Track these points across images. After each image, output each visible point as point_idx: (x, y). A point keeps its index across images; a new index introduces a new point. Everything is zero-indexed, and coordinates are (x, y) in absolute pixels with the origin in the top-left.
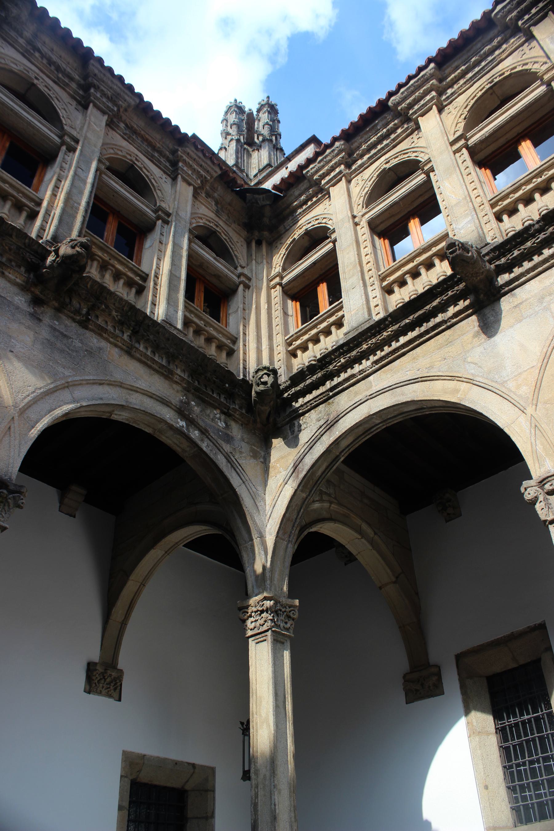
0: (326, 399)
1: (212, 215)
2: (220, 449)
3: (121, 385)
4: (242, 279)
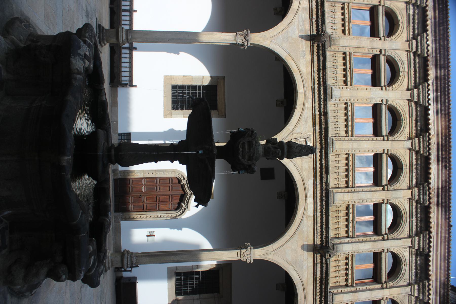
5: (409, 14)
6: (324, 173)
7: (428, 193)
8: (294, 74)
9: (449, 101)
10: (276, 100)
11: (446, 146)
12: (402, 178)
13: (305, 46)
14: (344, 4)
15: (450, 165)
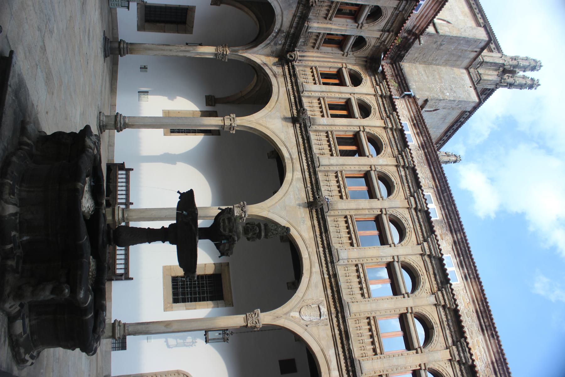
0: (284, 75)
1: (373, 44)
2: (271, 41)
3: (282, 13)
4: (346, 54)
5: (401, 176)
6: (344, 339)
7: (467, 349)
8: (296, 240)
9: (474, 263)
10: (287, 283)
11: (485, 311)
12: (435, 338)
13: (304, 213)
14: (337, 172)
15: (496, 332)
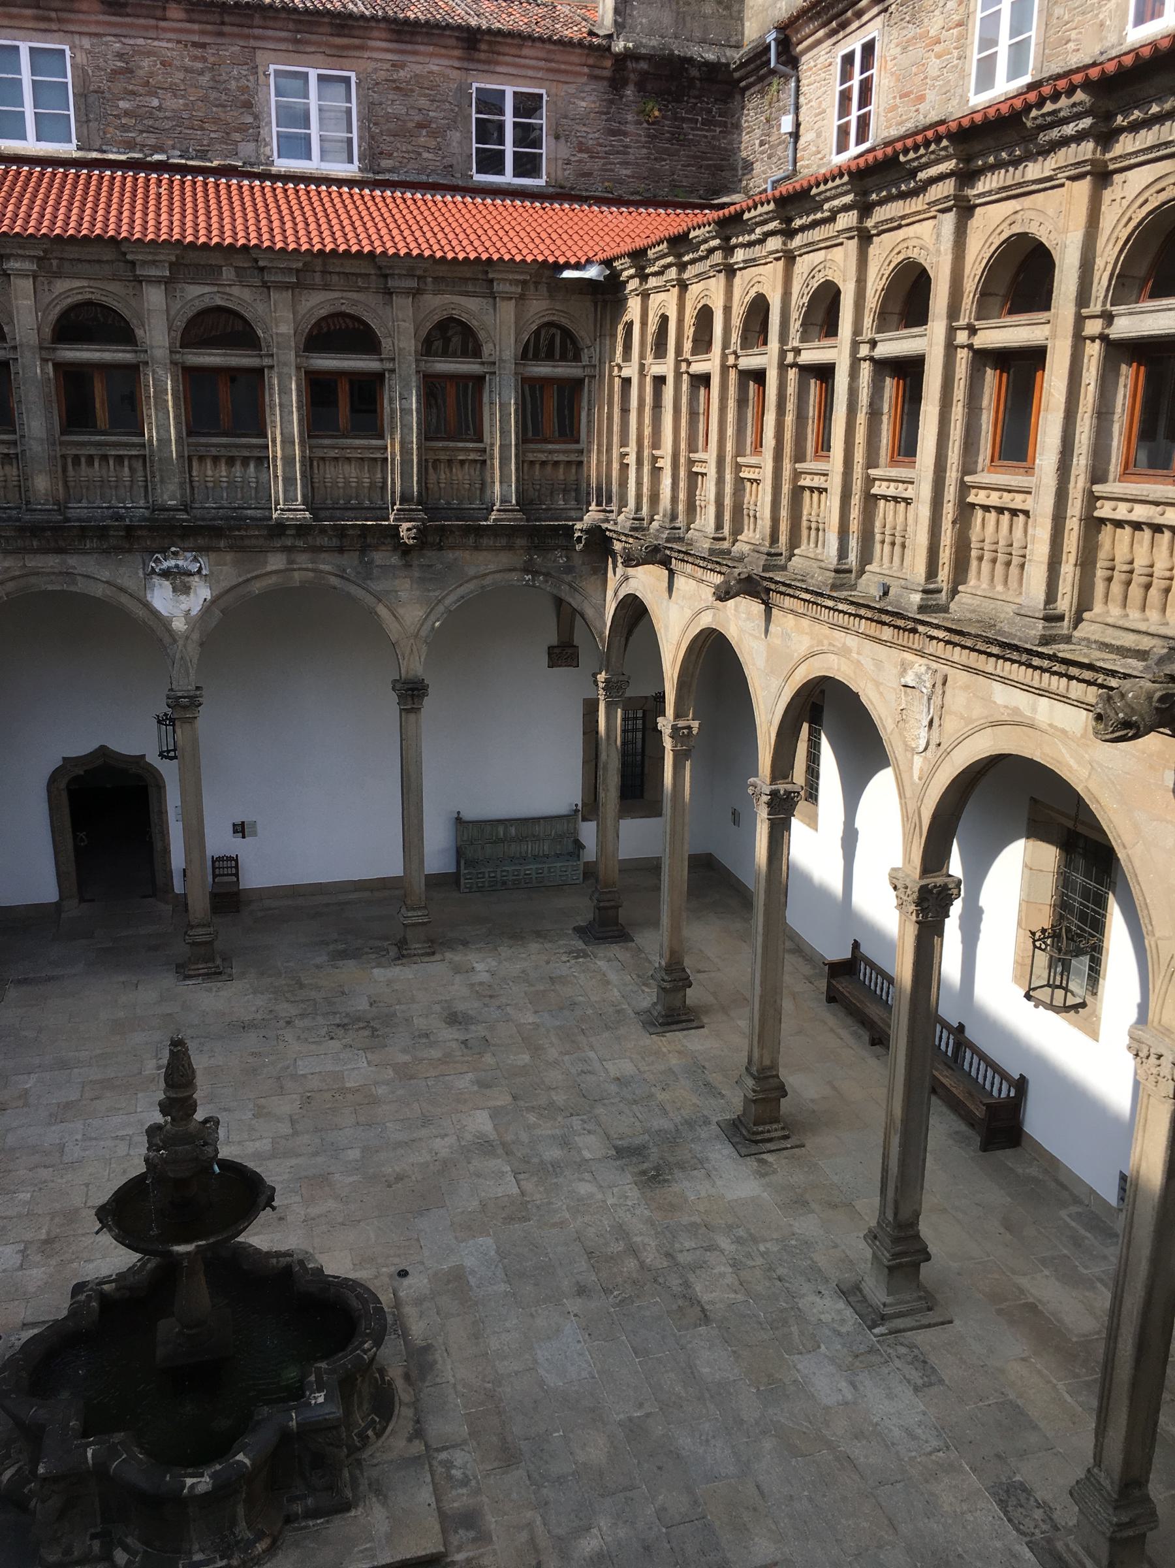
2: (563, 582)
3: (476, 577)
4: (588, 371)
